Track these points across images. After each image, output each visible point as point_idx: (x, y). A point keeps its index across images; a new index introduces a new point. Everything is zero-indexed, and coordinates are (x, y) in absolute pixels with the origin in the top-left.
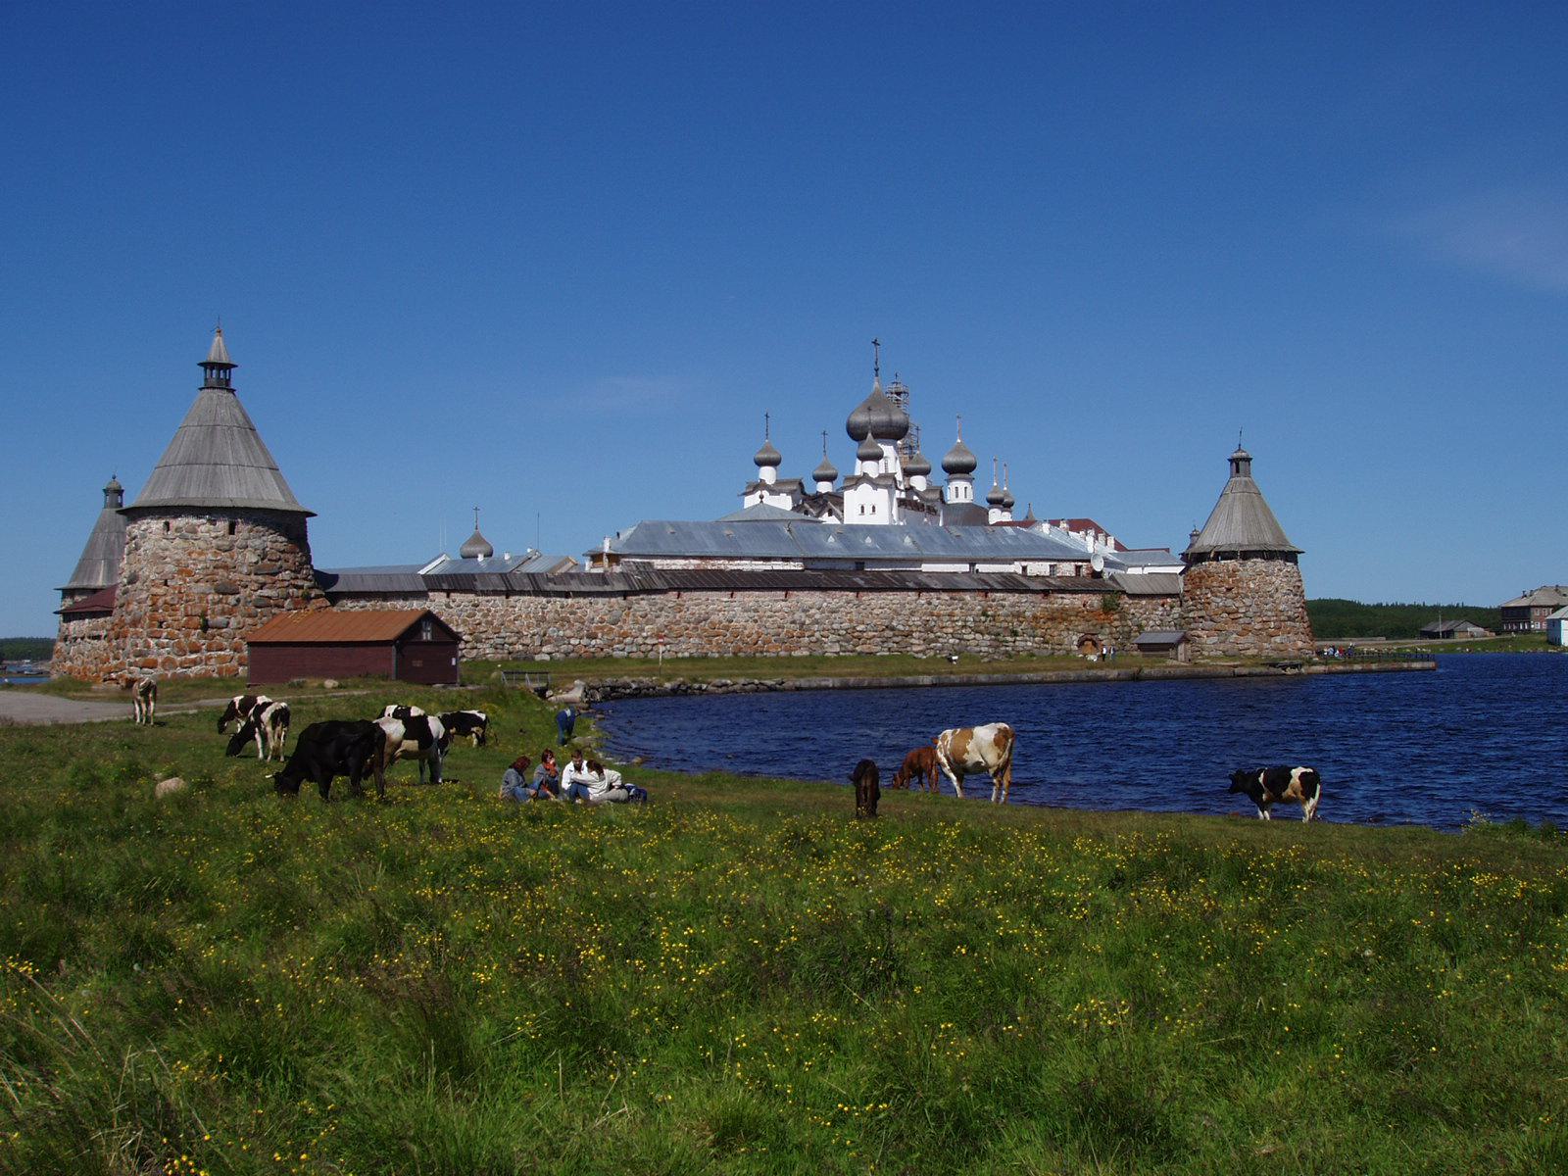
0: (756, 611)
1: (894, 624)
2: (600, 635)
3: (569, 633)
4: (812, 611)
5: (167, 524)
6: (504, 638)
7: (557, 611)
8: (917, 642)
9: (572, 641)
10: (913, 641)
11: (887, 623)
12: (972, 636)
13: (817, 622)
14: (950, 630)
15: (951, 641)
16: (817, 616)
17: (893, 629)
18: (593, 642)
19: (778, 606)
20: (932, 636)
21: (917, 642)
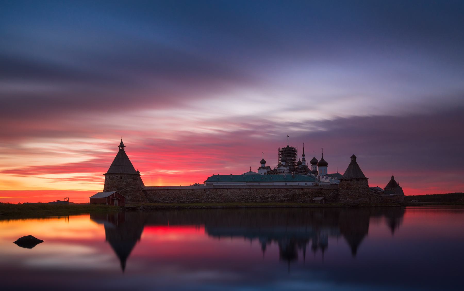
0: (233, 193)
1: (265, 196)
2: (199, 198)
3: (192, 198)
4: (246, 193)
5: (109, 177)
6: (179, 199)
7: (190, 193)
8: (270, 200)
9: (193, 199)
10: (269, 199)
11: (263, 196)
12: (283, 198)
13: (247, 195)
14: (278, 197)
15: (278, 199)
16: (247, 194)
17: (264, 197)
18: (198, 199)
19: (238, 192)
20: (273, 198)
21: (270, 200)
